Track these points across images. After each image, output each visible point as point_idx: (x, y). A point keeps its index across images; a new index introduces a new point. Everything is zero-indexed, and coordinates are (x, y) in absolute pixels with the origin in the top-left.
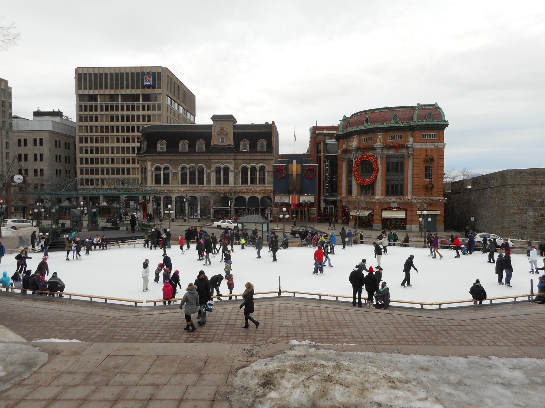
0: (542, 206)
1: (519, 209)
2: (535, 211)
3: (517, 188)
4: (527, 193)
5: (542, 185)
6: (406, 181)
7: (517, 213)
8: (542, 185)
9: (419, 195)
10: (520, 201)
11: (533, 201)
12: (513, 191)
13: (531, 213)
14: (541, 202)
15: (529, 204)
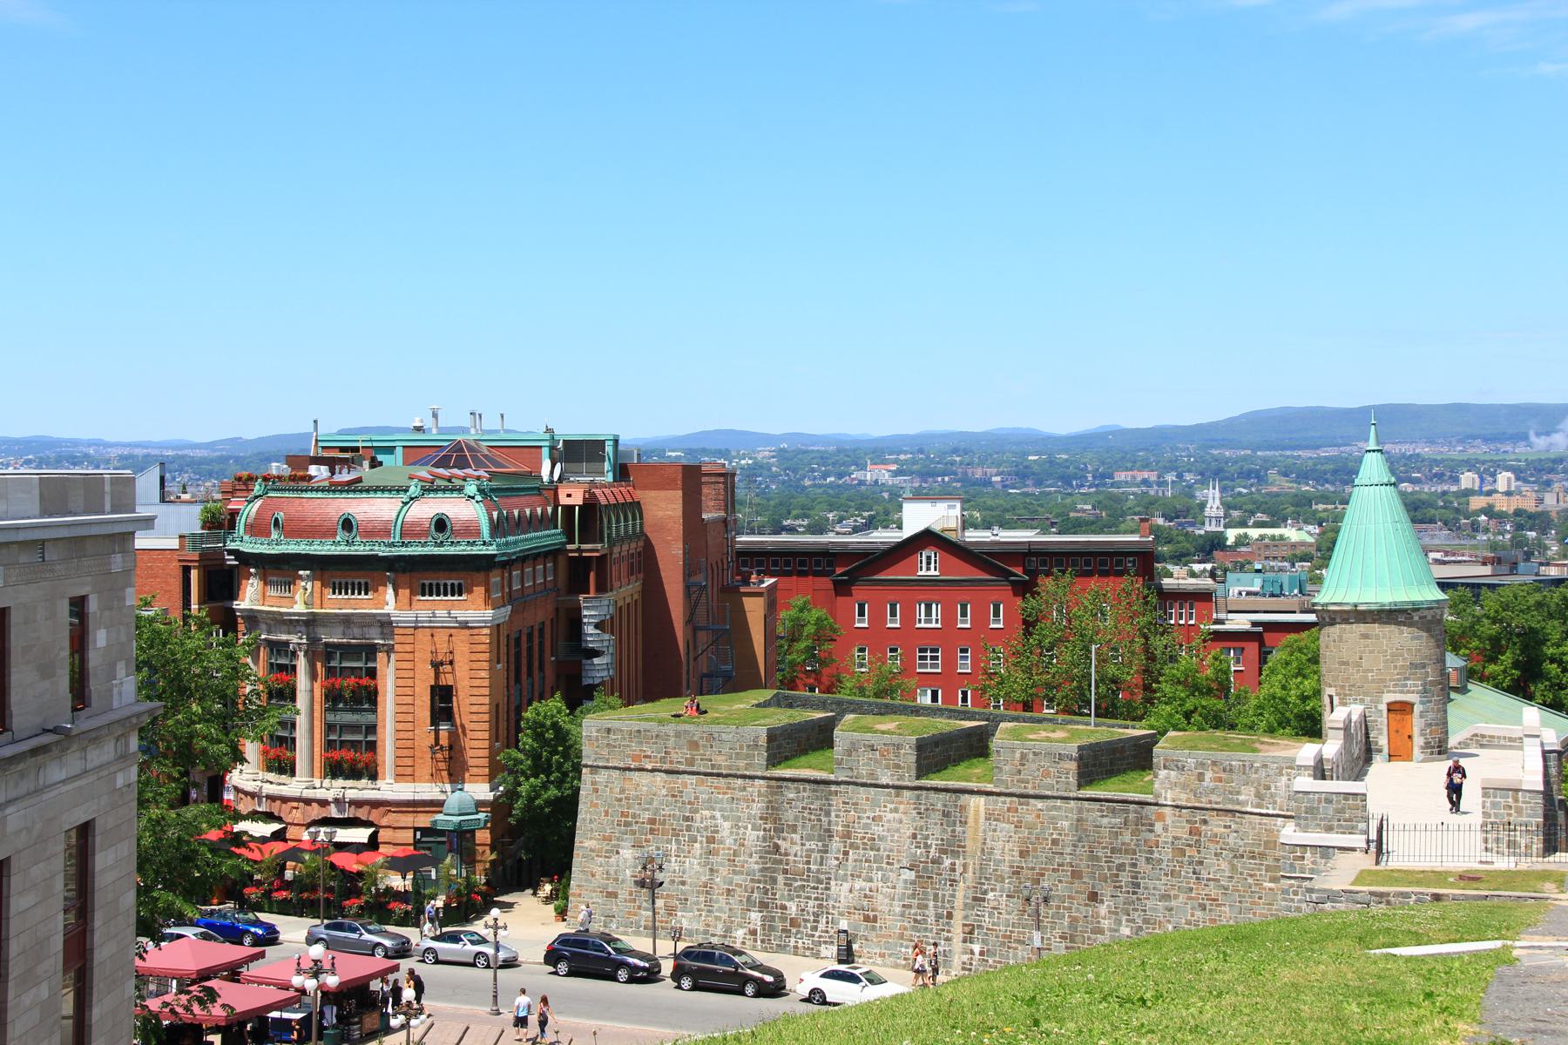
0: (652, 831)
1: (604, 839)
2: (637, 845)
3: (602, 777)
4: (622, 791)
5: (653, 771)
6: (379, 730)
7: (600, 850)
8: (653, 771)
9: (413, 777)
10: (607, 813)
11: (634, 816)
12: (593, 783)
13: (627, 853)
14: (652, 821)
15: (627, 824)
